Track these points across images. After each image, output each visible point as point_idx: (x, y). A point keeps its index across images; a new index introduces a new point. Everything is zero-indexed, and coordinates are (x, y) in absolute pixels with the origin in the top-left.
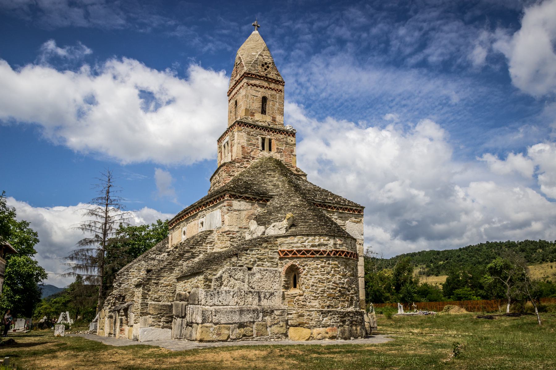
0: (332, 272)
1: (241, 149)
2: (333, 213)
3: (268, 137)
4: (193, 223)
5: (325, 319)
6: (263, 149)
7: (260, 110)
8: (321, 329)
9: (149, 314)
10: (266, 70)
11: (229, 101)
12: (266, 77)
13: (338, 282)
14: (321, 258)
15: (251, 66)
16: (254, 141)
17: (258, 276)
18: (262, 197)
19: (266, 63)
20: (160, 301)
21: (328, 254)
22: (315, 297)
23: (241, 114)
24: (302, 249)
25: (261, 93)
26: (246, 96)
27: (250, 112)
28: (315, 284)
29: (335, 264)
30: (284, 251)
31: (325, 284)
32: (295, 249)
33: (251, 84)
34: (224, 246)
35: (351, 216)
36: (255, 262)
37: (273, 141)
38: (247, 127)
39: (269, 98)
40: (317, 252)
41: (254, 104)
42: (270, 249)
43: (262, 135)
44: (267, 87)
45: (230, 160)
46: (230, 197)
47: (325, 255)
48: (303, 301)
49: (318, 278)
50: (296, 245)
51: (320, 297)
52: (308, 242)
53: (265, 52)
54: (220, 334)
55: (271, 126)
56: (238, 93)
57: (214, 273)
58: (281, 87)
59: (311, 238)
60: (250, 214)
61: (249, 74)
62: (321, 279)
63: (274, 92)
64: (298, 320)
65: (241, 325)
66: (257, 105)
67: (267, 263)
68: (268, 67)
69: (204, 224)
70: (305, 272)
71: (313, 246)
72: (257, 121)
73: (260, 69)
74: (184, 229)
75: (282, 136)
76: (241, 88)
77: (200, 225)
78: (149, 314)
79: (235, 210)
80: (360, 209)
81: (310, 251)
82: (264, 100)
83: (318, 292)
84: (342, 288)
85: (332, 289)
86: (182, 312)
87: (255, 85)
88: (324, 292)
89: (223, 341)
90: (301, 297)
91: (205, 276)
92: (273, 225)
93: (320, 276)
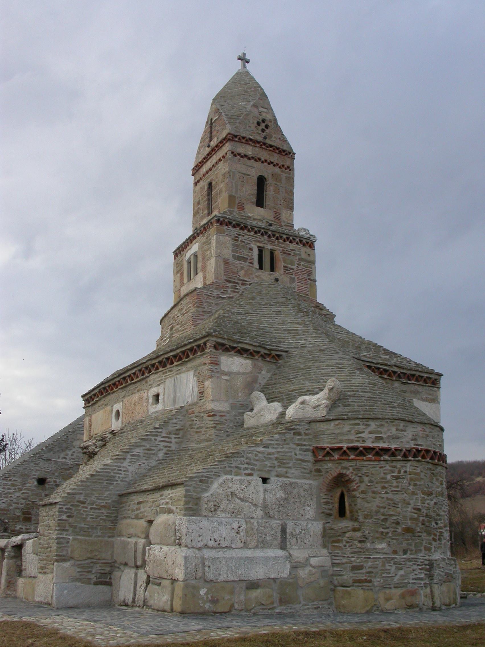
0: (411, 487)
1: (222, 264)
3: (269, 247)
4: (136, 396)
5: (402, 572)
6: (261, 268)
7: (254, 200)
8: (393, 591)
9: (72, 558)
10: (263, 131)
11: (196, 184)
12: (265, 144)
13: (419, 505)
14: (392, 461)
15: (240, 123)
16: (245, 253)
17: (281, 494)
18: (270, 350)
19: (263, 121)
20: (91, 536)
22: (382, 533)
23: (221, 206)
24: (359, 445)
25: (256, 170)
26: (230, 174)
28: (382, 510)
29: (416, 474)
30: (324, 449)
31: (398, 509)
32: (345, 445)
33: (239, 154)
34: (203, 437)
35: (420, 389)
37: (279, 255)
38: (234, 226)
39: (270, 181)
40: (385, 450)
42: (298, 445)
43: (259, 241)
44: (266, 161)
45: (200, 285)
46: (215, 347)
47: (399, 458)
48: (360, 542)
49: (387, 499)
50: (346, 438)
51: (390, 535)
52: (370, 433)
53: (261, 102)
54: (218, 600)
55: (273, 228)
56: (213, 169)
57: (204, 486)
59: (373, 425)
60: (249, 379)
61: (236, 136)
62: (392, 500)
63: (277, 170)
64: (351, 575)
65: (253, 585)
66: (250, 190)
67: (293, 471)
68: (267, 127)
69: (161, 397)
70: (363, 487)
71: (378, 439)
72: (250, 217)
73: (254, 129)
74: (118, 406)
75: (293, 246)
76: (220, 160)
77: (151, 401)
78: (72, 558)
80: (437, 377)
81: (373, 449)
82: (261, 181)
83: (387, 525)
84: (427, 516)
85: (411, 519)
86: (135, 558)
87: (246, 156)
88: (398, 523)
90: (357, 533)
91: (187, 491)
92: (301, 399)
93: (390, 496)
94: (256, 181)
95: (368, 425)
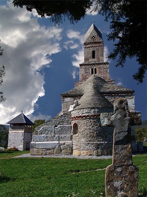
2: (116, 96)
3: (95, 68)
7: (92, 57)
10: (94, 39)
14: (86, 119)
19: (94, 36)
21: (90, 117)
27: (86, 59)
33: (87, 47)
36: (59, 123)
40: (84, 116)
41: (89, 55)
58: (101, 44)
61: (86, 43)
66: (91, 55)
71: (83, 114)
72: (91, 62)
79: (66, 102)
82: (93, 52)
87: (89, 47)
89: (40, 155)
93: (86, 127)
94: (92, 52)
95: (81, 111)
